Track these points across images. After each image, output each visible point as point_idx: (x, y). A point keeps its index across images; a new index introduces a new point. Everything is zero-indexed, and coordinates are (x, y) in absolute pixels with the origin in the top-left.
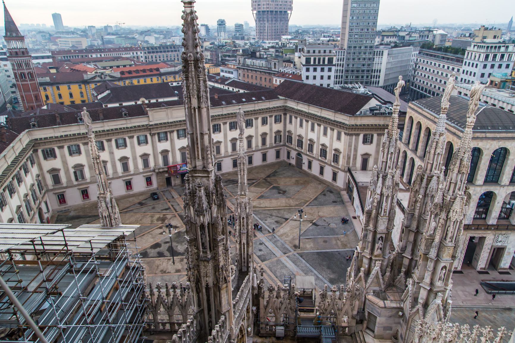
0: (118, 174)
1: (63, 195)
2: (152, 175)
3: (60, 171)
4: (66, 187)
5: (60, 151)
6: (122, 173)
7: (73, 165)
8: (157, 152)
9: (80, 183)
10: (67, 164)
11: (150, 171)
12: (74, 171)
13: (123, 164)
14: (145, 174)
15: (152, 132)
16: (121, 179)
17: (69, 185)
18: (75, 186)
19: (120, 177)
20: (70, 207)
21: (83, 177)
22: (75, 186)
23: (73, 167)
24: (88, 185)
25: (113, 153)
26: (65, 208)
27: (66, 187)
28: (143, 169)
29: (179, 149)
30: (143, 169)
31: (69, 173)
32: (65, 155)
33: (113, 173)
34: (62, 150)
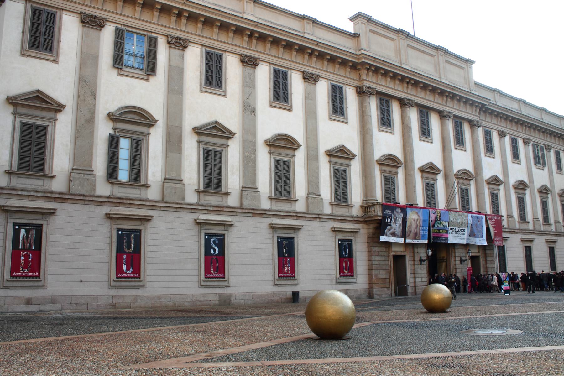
0: (259, 200)
1: (39, 229)
3: (61, 117)
4: (61, 198)
5: (83, 35)
7: (113, 107)
8: (373, 155)
9: (120, 192)
10: (94, 95)
12: (112, 132)
14: (339, 225)
15: (367, 84)
16: (265, 222)
17: (77, 188)
18: (100, 202)
19: (258, 213)
20: (53, 301)
22: (100, 202)
23: (111, 117)
24: (150, 213)
25: (253, 111)
26: (28, 302)
27: (61, 198)
30: (331, 204)
31: (92, 134)
32: (95, 58)
34: (92, 32)
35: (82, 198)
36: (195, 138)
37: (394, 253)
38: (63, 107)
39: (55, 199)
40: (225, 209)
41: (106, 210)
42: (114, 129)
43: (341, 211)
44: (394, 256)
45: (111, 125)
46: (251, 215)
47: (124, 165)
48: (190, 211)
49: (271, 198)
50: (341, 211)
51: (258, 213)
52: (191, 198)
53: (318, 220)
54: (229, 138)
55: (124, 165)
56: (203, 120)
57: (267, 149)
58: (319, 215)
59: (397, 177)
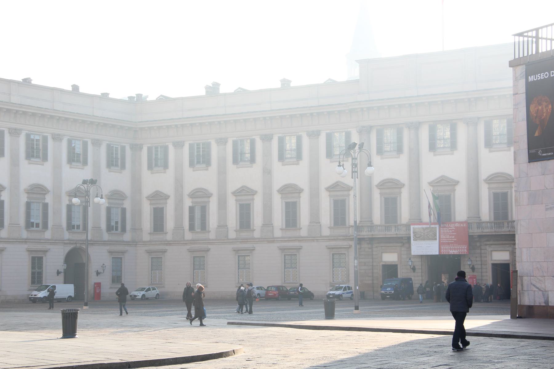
2: (350, 246)
6: (281, 229)
11: (347, 238)
12: (191, 205)
13: (287, 204)
21: (204, 226)
24: (210, 246)
28: (330, 228)
29: (430, 184)
30: (330, 228)
33: (264, 225)
35: (176, 242)
36: (234, 198)
37: (384, 263)
38: (169, 197)
39: (167, 244)
40: (249, 241)
41: (188, 247)
42: (192, 202)
43: (341, 232)
44: (383, 266)
45: (191, 200)
46: (266, 242)
47: (197, 222)
48: (230, 243)
49: (281, 229)
50: (341, 232)
51: (272, 240)
52: (232, 235)
53: (315, 241)
54: (254, 195)
55: (197, 222)
56: (238, 186)
57: (280, 196)
58: (314, 237)
59: (400, 196)
